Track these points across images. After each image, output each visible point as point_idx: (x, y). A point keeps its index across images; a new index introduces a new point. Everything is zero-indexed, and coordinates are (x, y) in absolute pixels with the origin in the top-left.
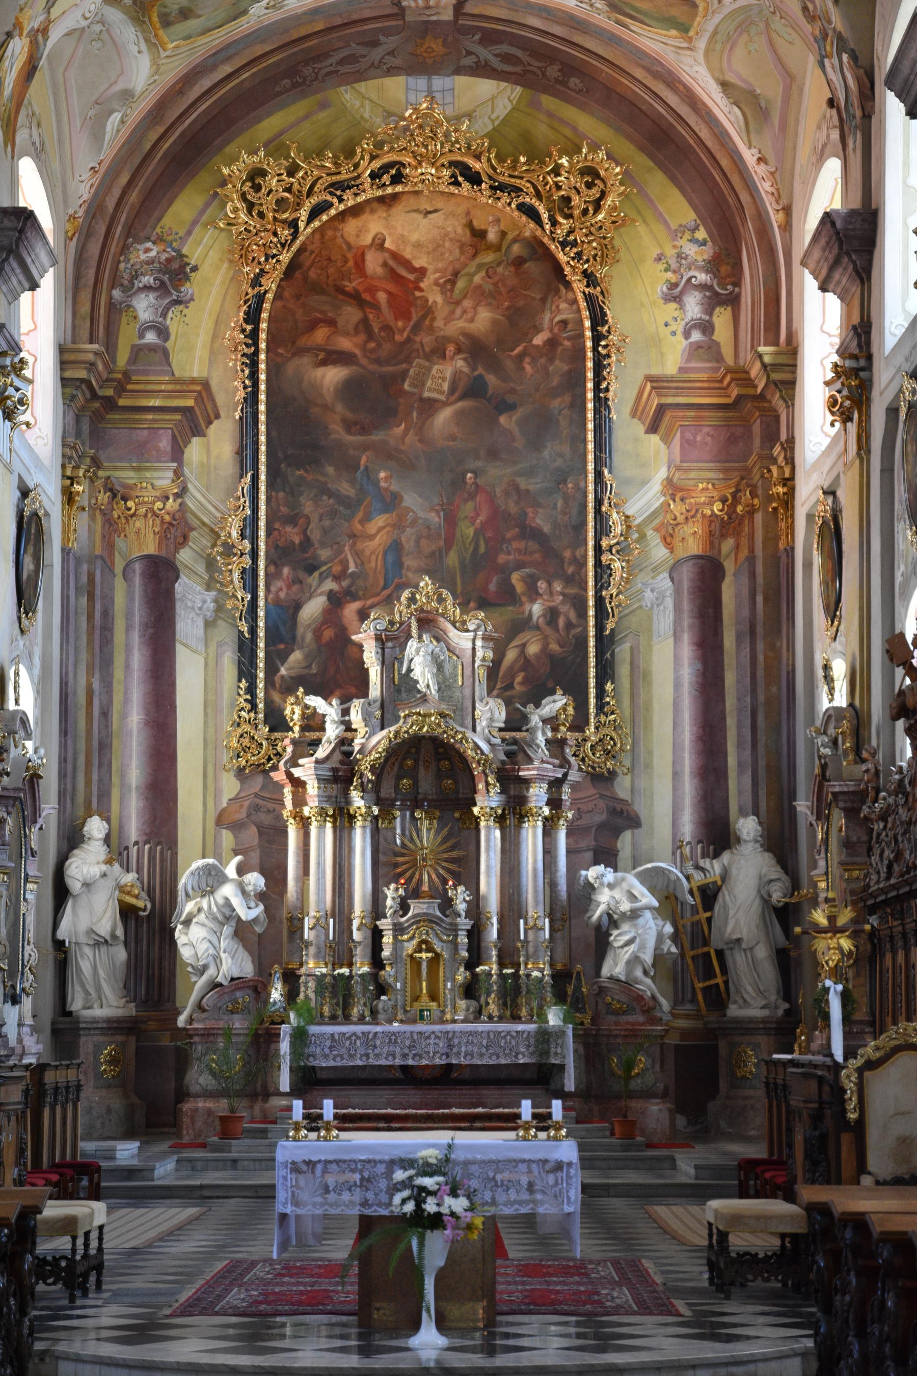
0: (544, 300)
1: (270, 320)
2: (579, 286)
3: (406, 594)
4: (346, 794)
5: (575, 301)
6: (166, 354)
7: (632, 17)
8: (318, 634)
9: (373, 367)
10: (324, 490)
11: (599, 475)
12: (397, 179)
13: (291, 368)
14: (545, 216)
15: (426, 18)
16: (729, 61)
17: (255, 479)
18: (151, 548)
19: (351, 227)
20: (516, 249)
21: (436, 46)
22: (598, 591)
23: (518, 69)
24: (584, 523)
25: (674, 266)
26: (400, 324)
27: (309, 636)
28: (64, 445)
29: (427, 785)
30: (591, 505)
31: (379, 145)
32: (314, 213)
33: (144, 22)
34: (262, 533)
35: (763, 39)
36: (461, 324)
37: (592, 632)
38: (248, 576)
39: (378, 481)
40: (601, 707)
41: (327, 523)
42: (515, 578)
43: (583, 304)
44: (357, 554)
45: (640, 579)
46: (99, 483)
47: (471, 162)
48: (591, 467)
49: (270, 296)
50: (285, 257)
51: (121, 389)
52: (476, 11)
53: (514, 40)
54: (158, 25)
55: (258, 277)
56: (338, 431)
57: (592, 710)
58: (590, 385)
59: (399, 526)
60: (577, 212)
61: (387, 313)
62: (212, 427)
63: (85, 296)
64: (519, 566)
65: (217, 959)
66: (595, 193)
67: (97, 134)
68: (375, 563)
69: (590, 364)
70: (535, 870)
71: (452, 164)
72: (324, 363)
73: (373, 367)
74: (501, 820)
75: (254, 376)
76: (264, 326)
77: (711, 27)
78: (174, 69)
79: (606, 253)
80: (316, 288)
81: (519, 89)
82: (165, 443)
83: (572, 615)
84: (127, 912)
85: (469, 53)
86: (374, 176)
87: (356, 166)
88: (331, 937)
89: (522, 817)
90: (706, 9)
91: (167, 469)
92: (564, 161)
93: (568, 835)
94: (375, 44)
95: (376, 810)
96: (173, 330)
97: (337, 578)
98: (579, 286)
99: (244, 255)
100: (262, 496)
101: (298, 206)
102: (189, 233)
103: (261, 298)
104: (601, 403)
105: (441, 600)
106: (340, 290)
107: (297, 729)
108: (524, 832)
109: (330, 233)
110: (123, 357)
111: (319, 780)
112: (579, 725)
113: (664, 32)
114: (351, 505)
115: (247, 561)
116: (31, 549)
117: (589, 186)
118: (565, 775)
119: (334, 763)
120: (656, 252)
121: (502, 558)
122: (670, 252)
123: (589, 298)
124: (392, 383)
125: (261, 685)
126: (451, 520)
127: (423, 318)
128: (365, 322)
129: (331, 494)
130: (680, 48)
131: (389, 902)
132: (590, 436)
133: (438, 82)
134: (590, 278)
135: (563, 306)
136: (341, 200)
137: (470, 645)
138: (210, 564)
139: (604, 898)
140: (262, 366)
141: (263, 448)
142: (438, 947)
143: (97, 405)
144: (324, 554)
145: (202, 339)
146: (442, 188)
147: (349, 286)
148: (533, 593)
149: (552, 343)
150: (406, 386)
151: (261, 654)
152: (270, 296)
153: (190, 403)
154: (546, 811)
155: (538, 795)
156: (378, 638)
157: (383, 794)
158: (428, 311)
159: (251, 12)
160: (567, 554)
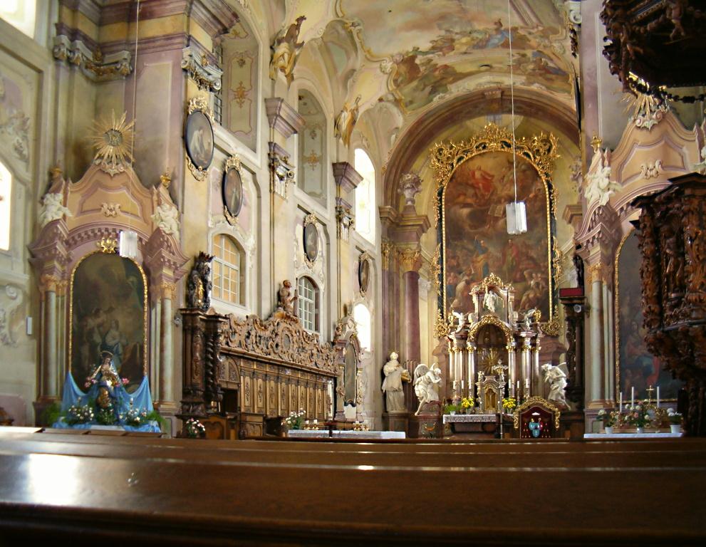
0: (532, 183)
1: (446, 195)
2: (543, 177)
3: (486, 279)
4: (465, 343)
5: (543, 183)
6: (414, 208)
8: (462, 293)
9: (479, 208)
10: (463, 247)
11: (552, 238)
12: (484, 148)
13: (452, 210)
14: (532, 156)
17: (442, 245)
18: (411, 269)
19: (471, 163)
20: (523, 167)
21: (496, 106)
22: (552, 276)
23: (522, 111)
24: (548, 254)
25: (575, 168)
26: (487, 193)
27: (460, 294)
28: (382, 238)
29: (493, 340)
30: (549, 249)
31: (478, 138)
32: (459, 160)
34: (444, 263)
36: (506, 192)
37: (550, 289)
38: (440, 276)
39: (481, 244)
40: (553, 314)
41: (465, 258)
42: (525, 272)
43: (545, 183)
44: (475, 268)
45: (566, 273)
46: (395, 249)
47: (507, 141)
48: (549, 236)
49: (445, 187)
50: (450, 175)
51: (401, 220)
55: (441, 182)
56: (467, 228)
57: (551, 315)
58: (548, 209)
59: (487, 258)
60: (542, 154)
61: (482, 191)
62: (429, 230)
63: (389, 193)
64: (526, 269)
65: (426, 395)
66: (547, 147)
67: (389, 142)
68: (480, 270)
69: (548, 203)
70: (526, 366)
71: (501, 142)
72: (462, 207)
73: (479, 208)
74: (515, 350)
75: (441, 213)
76: (443, 197)
78: (413, 120)
79: (553, 165)
80: (460, 184)
81: (522, 117)
82: (414, 235)
83: (544, 284)
84: (404, 382)
85: (506, 107)
86: (477, 147)
87: (471, 145)
88: (463, 387)
89: (522, 350)
91: (414, 244)
92: (536, 138)
93: (539, 355)
94: (476, 107)
95: (475, 348)
96: (416, 200)
97: (468, 276)
98: (543, 177)
99: (438, 175)
100: (444, 251)
101: (453, 158)
102: (420, 170)
103: (442, 189)
104: (552, 215)
105: (497, 281)
106: (467, 184)
107: (452, 323)
108: (524, 354)
109: (463, 167)
110: (401, 209)
111: (457, 338)
112: (545, 317)
114: (472, 252)
115: (439, 272)
116: (364, 271)
117: (545, 145)
118: (537, 335)
119: (462, 333)
120: (569, 166)
121: (521, 267)
122: (574, 165)
123: (548, 182)
124: (484, 212)
125: (445, 310)
126: (504, 255)
127: (493, 191)
128: (476, 194)
129: (465, 249)
131: (479, 377)
132: (549, 226)
133: (497, 117)
134: (547, 175)
135: (539, 184)
136: (466, 156)
137: (506, 295)
138: (429, 273)
139: (548, 374)
140: (443, 210)
141: (444, 235)
142: (494, 391)
143: (394, 226)
144: (464, 268)
145: (425, 201)
146: (499, 149)
147: (470, 182)
148: (531, 278)
149: (536, 196)
150: (489, 213)
151: (445, 301)
152: (445, 187)
153: (422, 223)
154: (530, 347)
155: (527, 342)
156: (477, 293)
157: (479, 343)
158: (495, 189)
160: (542, 264)
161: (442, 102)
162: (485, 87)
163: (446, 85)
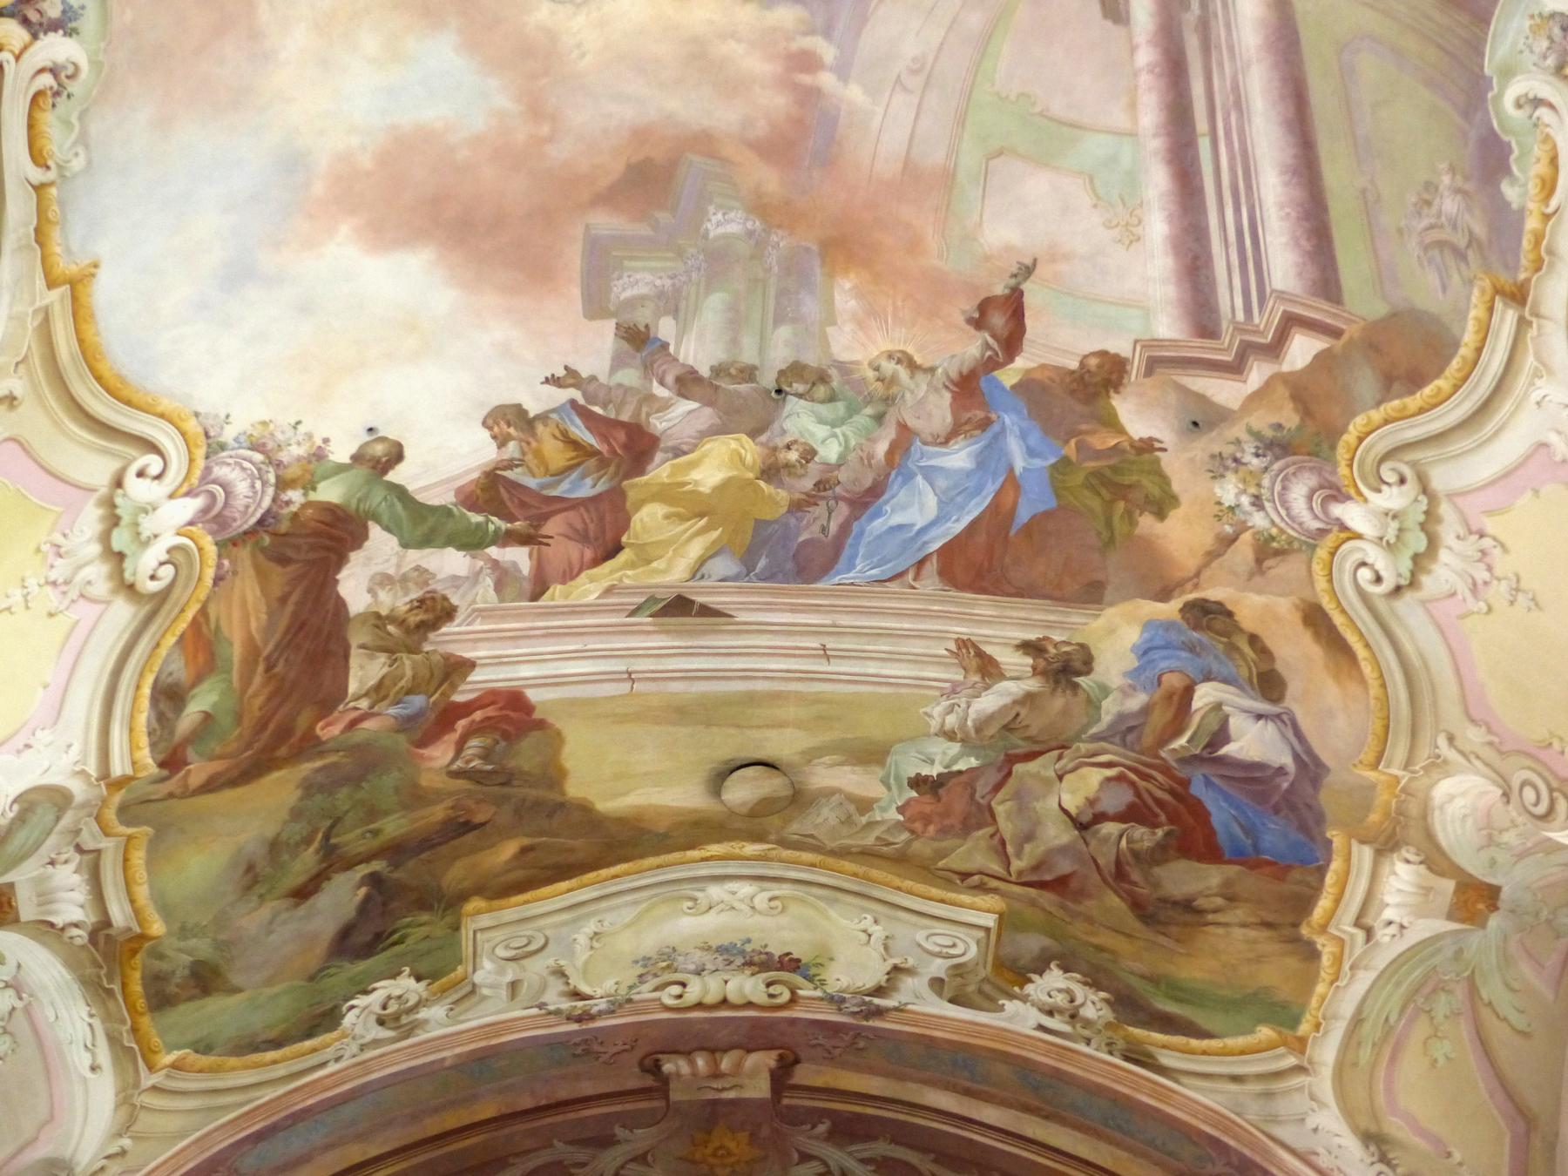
7: (1168, 1024)
15: (711, 1095)
16: (1389, 1090)
33: (110, 993)
35: (1465, 1030)
52: (819, 1082)
53: (902, 1134)
54: (141, 1003)
77: (1347, 1007)
85: (805, 1157)
90: (1338, 960)
94: (607, 1142)
113: (1240, 1041)
130: (1278, 1075)
159: (349, 1019)
161: (397, 1058)
162: (693, 993)
163: (464, 897)
